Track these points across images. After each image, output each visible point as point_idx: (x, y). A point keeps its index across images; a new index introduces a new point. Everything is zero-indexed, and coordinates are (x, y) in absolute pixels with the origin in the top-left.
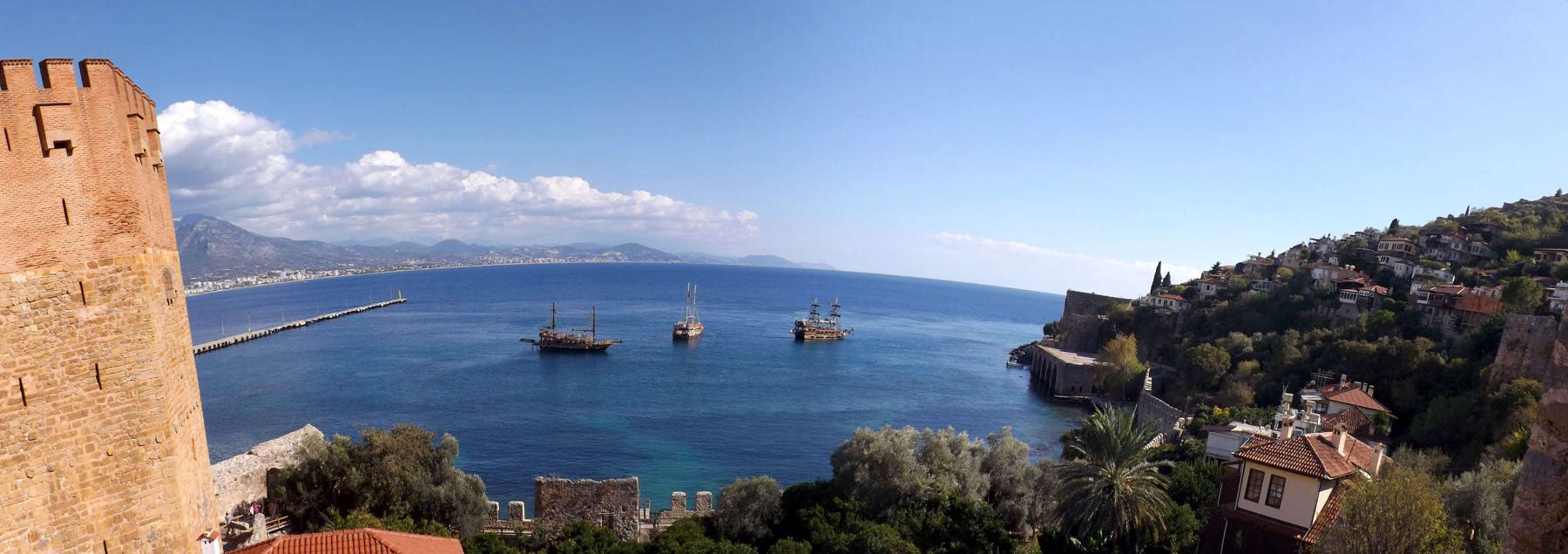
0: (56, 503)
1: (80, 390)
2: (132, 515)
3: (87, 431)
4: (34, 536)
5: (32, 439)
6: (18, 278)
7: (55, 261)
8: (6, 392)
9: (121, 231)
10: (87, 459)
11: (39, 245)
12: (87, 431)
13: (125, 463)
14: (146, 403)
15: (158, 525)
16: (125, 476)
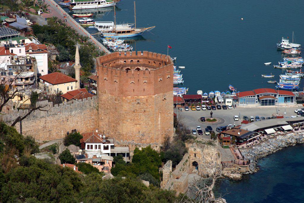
0: (109, 122)
1: (114, 110)
2: (117, 128)
3: (113, 115)
4: (106, 124)
5: (107, 114)
6: (109, 95)
7: (113, 95)
8: (106, 107)
9: (121, 94)
10: (113, 119)
11: (112, 92)
12: (113, 115)
13: (117, 122)
14: (121, 116)
15: (120, 131)
16: (117, 123)
